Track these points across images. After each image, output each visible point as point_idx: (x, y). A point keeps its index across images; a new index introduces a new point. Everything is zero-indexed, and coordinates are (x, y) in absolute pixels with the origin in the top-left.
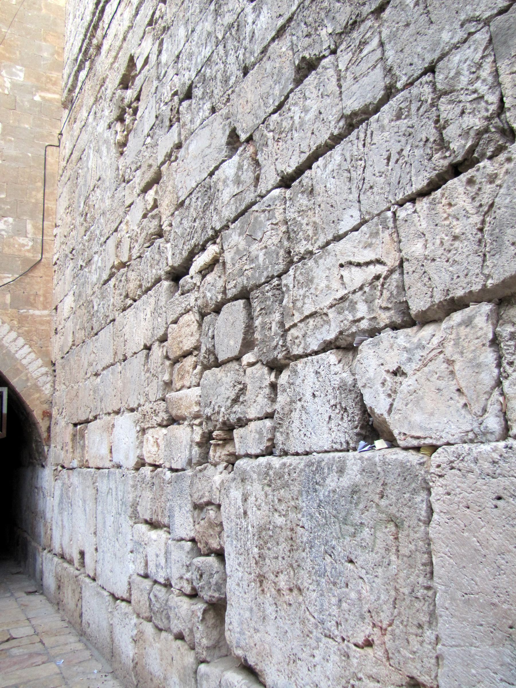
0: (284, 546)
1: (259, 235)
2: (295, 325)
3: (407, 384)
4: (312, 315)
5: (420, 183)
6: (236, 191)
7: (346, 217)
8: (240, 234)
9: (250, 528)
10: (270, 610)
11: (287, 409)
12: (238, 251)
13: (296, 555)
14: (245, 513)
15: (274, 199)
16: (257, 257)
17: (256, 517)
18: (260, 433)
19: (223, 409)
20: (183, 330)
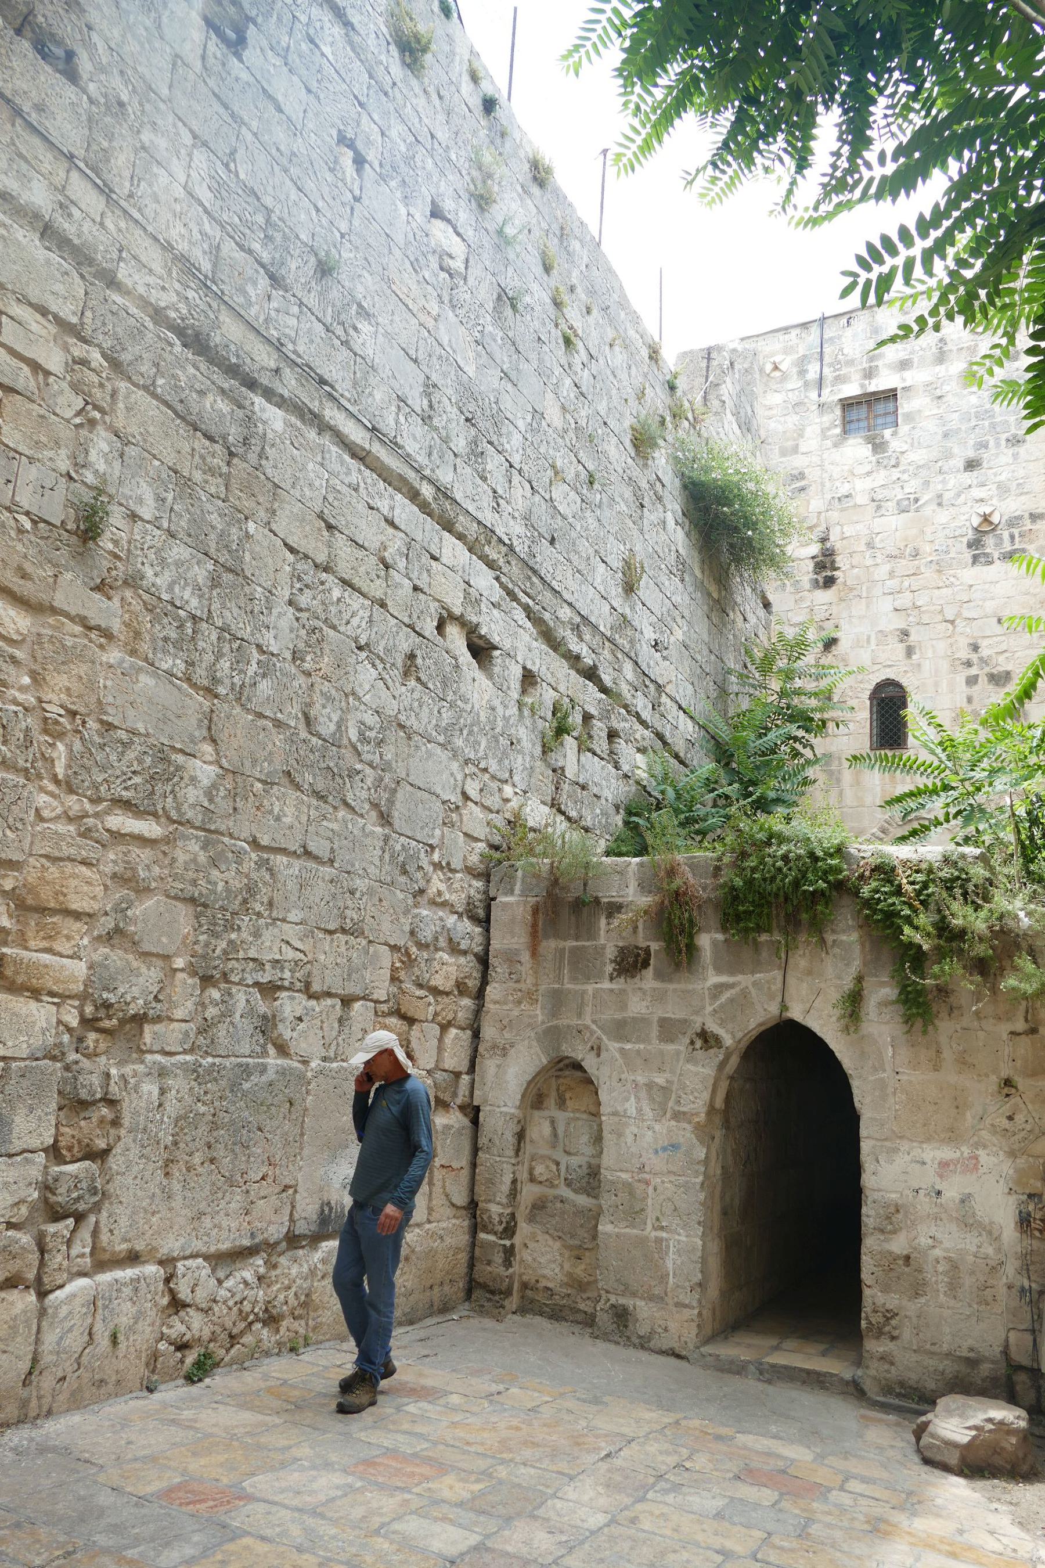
0: (203, 1129)
1: (223, 867)
2: (237, 959)
3: (302, 1025)
4: (253, 960)
5: (331, 927)
6: (206, 804)
7: (294, 912)
8: (202, 848)
9: (166, 1119)
10: (176, 1186)
11: (216, 1020)
12: (194, 860)
13: (215, 1134)
14: (160, 1105)
15: (246, 852)
16: (216, 884)
17: (172, 1107)
18: (186, 1034)
19: (141, 1002)
20: (73, 883)
